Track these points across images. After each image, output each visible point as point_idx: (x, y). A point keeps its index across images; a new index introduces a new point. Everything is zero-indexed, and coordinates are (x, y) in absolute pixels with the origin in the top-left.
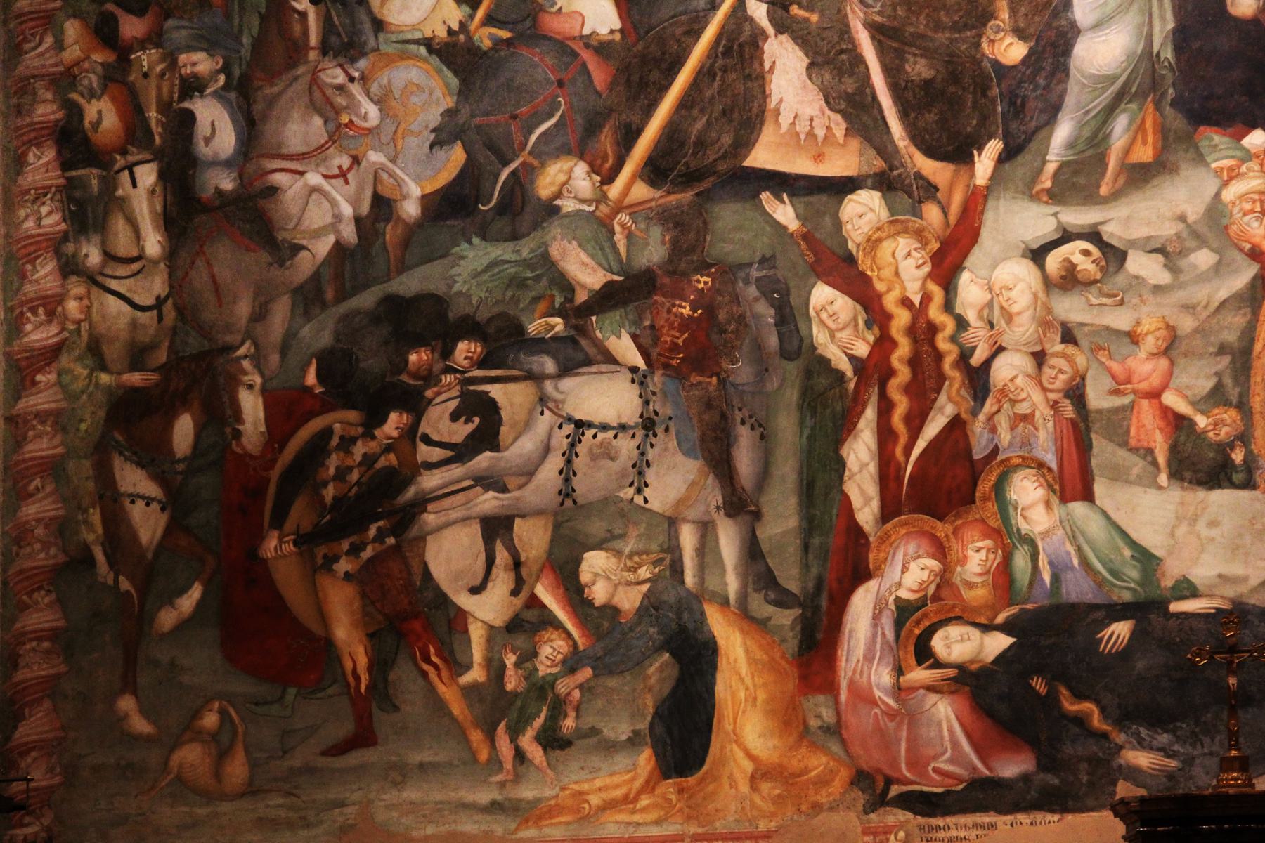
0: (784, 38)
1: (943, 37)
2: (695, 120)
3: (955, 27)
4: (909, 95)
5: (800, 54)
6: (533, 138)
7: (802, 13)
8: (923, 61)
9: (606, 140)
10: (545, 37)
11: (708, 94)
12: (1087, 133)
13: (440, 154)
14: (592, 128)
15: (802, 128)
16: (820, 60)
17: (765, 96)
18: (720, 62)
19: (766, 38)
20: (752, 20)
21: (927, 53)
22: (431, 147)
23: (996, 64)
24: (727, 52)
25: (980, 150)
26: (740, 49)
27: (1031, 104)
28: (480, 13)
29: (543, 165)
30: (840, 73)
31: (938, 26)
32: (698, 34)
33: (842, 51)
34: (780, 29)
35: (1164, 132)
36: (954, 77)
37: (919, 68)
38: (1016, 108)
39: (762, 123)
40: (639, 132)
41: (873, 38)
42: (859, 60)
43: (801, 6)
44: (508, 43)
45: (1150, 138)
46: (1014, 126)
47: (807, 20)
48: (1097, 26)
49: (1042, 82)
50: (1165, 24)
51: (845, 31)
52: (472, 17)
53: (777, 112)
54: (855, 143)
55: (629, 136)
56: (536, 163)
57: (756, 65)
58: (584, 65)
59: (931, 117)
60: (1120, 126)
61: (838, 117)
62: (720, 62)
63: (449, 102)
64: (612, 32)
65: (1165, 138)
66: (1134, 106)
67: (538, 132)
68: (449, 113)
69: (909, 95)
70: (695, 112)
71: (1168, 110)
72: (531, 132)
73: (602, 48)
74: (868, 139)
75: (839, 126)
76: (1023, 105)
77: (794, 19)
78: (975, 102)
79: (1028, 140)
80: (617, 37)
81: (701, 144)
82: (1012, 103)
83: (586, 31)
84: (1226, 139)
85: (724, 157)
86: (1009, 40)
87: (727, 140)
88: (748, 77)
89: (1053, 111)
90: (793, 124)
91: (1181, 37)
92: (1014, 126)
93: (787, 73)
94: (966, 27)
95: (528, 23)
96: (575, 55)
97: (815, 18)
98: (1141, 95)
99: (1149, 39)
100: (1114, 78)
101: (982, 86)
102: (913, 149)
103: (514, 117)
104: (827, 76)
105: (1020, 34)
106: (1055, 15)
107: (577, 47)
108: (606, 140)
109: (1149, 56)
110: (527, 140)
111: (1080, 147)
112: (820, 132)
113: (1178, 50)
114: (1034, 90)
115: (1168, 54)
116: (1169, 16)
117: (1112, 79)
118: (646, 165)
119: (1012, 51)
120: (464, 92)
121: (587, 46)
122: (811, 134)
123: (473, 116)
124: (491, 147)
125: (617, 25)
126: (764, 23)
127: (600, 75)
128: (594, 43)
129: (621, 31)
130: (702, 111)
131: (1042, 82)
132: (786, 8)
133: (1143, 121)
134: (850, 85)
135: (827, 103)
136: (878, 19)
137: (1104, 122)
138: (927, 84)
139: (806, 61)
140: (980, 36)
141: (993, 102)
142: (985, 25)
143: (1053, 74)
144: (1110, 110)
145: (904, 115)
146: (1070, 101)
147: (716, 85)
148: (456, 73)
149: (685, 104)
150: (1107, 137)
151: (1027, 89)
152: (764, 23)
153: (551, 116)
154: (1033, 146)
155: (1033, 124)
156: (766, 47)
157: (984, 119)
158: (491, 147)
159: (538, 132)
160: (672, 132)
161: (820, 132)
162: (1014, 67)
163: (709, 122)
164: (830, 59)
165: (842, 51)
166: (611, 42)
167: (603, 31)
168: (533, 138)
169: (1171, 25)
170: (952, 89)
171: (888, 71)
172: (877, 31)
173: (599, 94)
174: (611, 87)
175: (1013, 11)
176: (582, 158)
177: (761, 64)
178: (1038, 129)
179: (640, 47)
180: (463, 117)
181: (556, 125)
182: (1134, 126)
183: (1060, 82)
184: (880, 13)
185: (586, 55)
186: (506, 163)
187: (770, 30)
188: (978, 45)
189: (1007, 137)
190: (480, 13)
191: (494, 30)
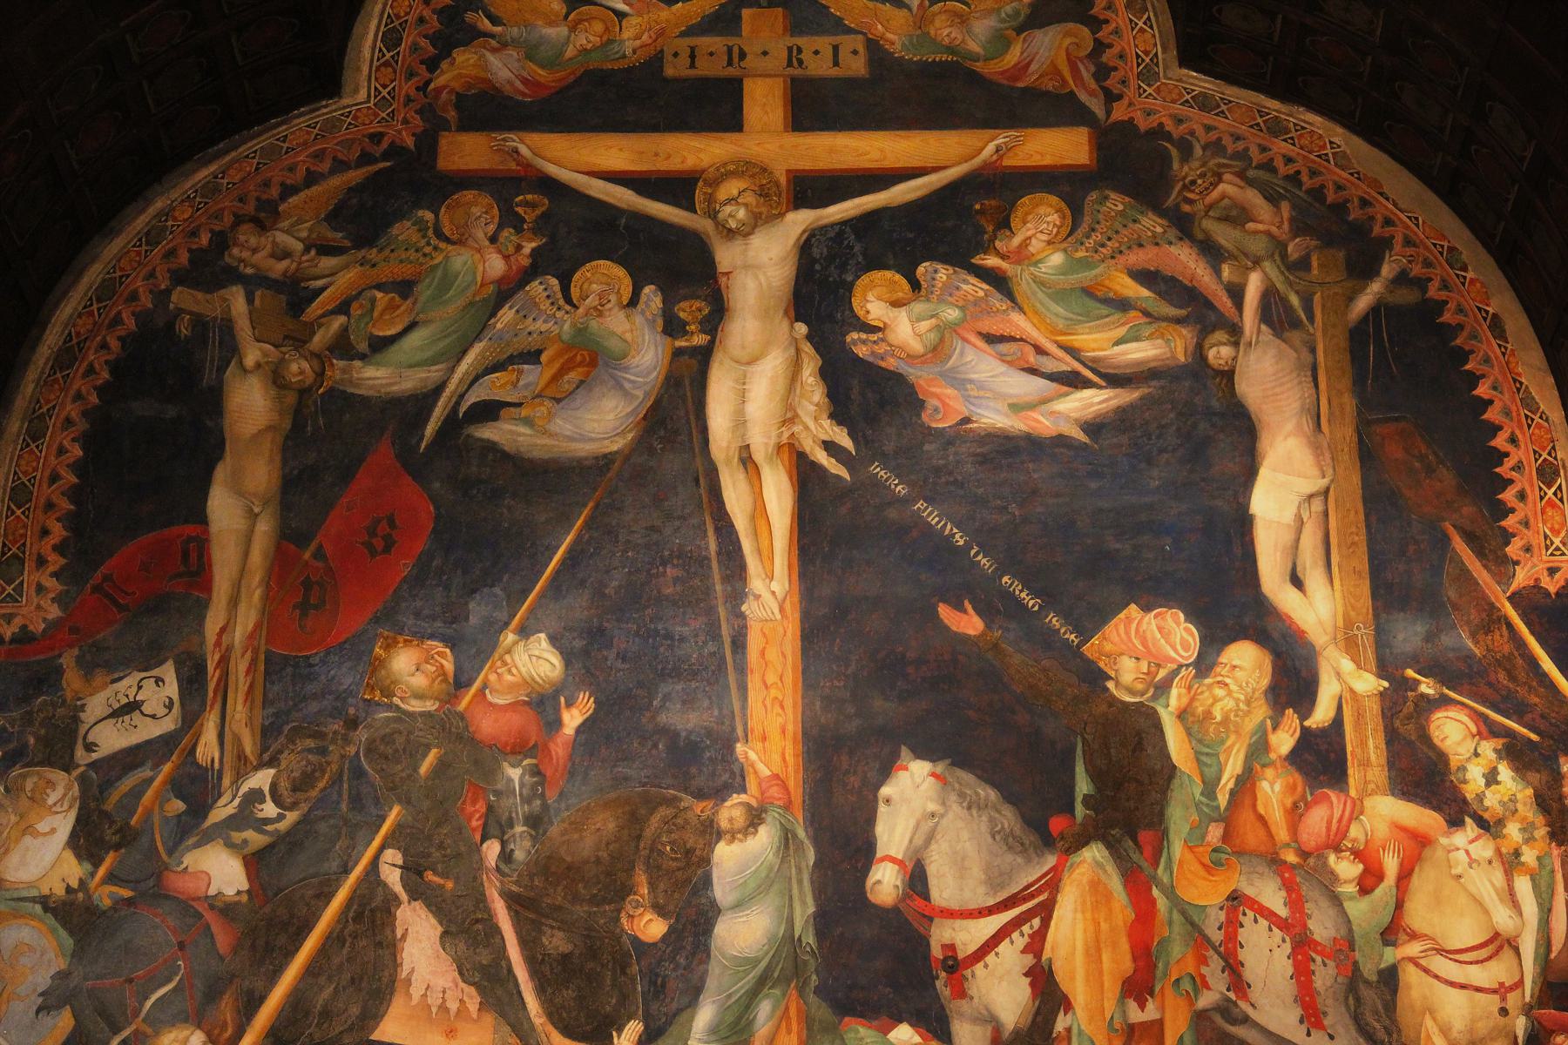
0: (417, 904)
1: (580, 910)
2: (321, 989)
3: (594, 900)
4: (546, 969)
5: (433, 921)
6: (149, 1004)
7: (436, 879)
8: (561, 934)
9: (226, 1009)
10: (167, 897)
11: (336, 961)
12: (730, 1019)
13: (47, 1020)
14: (212, 994)
15: (434, 1000)
16: (453, 929)
17: (396, 965)
18: (351, 927)
19: (400, 904)
20: (385, 885)
21: (565, 926)
22: (37, 1012)
23: (636, 941)
24: (358, 918)
25: (620, 1031)
26: (372, 918)
27: (671, 985)
28: (102, 871)
29: (157, 1034)
30: (474, 943)
31: (576, 899)
32: (329, 897)
33: (477, 921)
34: (414, 895)
35: (808, 1021)
36: (593, 953)
37: (556, 942)
38: (657, 988)
39: (392, 994)
40: (262, 999)
41: (509, 908)
42: (497, 931)
43: (435, 873)
44: (129, 902)
45: (795, 1027)
46: (654, 1007)
47: (443, 886)
48: (738, 906)
49: (682, 961)
50: (804, 909)
51: (481, 901)
52: (93, 875)
53: (408, 982)
54: (489, 1019)
55: (252, 1003)
56: (149, 1031)
57: (388, 932)
58: (208, 927)
59: (569, 993)
60: (764, 1010)
61: (472, 990)
62: (351, 927)
63: (62, 964)
64: (239, 893)
65: (809, 1029)
66: (777, 992)
67: (154, 998)
68: (62, 976)
69: (546, 969)
70: (322, 980)
71: (812, 998)
72: (146, 998)
73: (227, 910)
74: (503, 1015)
75: (473, 1002)
76: (663, 985)
77: (429, 883)
78: (614, 980)
79: (669, 1023)
80: (245, 898)
81: (326, 1014)
82: (653, 983)
83: (212, 891)
84: (871, 1032)
85: (351, 1029)
86: (648, 917)
87: (355, 1010)
88: (380, 944)
89: (694, 993)
90: (425, 995)
91: (823, 921)
92: (654, 1007)
93: (420, 943)
94: (604, 901)
95: (151, 882)
96: (200, 916)
97: (450, 885)
98: (784, 980)
99: (790, 922)
100: (757, 961)
101: (622, 966)
102: (550, 1028)
103: (131, 981)
104: (462, 946)
105: (660, 910)
106: (695, 892)
107: (201, 908)
108: (226, 1009)
109: (790, 941)
110: (142, 1005)
111: (723, 1034)
112: (453, 1006)
113: (820, 934)
114: (674, 970)
115: (810, 939)
116: (810, 900)
117: (755, 962)
118: (267, 1036)
119: (652, 928)
120: (78, 954)
121: (212, 907)
122: (443, 1008)
123: (85, 978)
124: (102, 1012)
125: (245, 886)
126: (398, 888)
127: (223, 939)
128: (219, 904)
129: (248, 892)
130: (330, 979)
131: (682, 961)
132: (420, 874)
133: (787, 1009)
134: (485, 957)
135: (461, 973)
136: (514, 888)
137: (748, 1007)
138: (565, 958)
139: (440, 929)
140: (619, 911)
141: (633, 980)
142: (624, 899)
143: (693, 954)
144: (754, 994)
145: (541, 990)
146: (711, 984)
147: (345, 951)
148: (71, 933)
149: (312, 971)
150: (751, 1023)
151: (667, 969)
152: (398, 888)
153: (169, 980)
154: (674, 1030)
155: (674, 1006)
156: (398, 913)
157: (624, 998)
158: (102, 1012)
159: (154, 998)
160: (296, 1004)
161: (453, 1006)
162: (655, 944)
163: (336, 991)
164: (465, 929)
165: (477, 921)
166: (237, 903)
167: (230, 892)
168: (149, 1004)
169: (811, 909)
170: (591, 965)
171: (523, 942)
172: (512, 900)
173: (222, 958)
174: (235, 951)
175: (652, 886)
176: (199, 1027)
177: (393, 931)
178: (680, 1011)
179: (267, 909)
180: (74, 981)
181: (174, 990)
182: (779, 1013)
183: (701, 962)
184: (517, 883)
185: (209, 916)
186: (116, 1030)
187: (404, 896)
188: (618, 919)
189: (647, 1019)
190: (102, 871)
191: (114, 889)
